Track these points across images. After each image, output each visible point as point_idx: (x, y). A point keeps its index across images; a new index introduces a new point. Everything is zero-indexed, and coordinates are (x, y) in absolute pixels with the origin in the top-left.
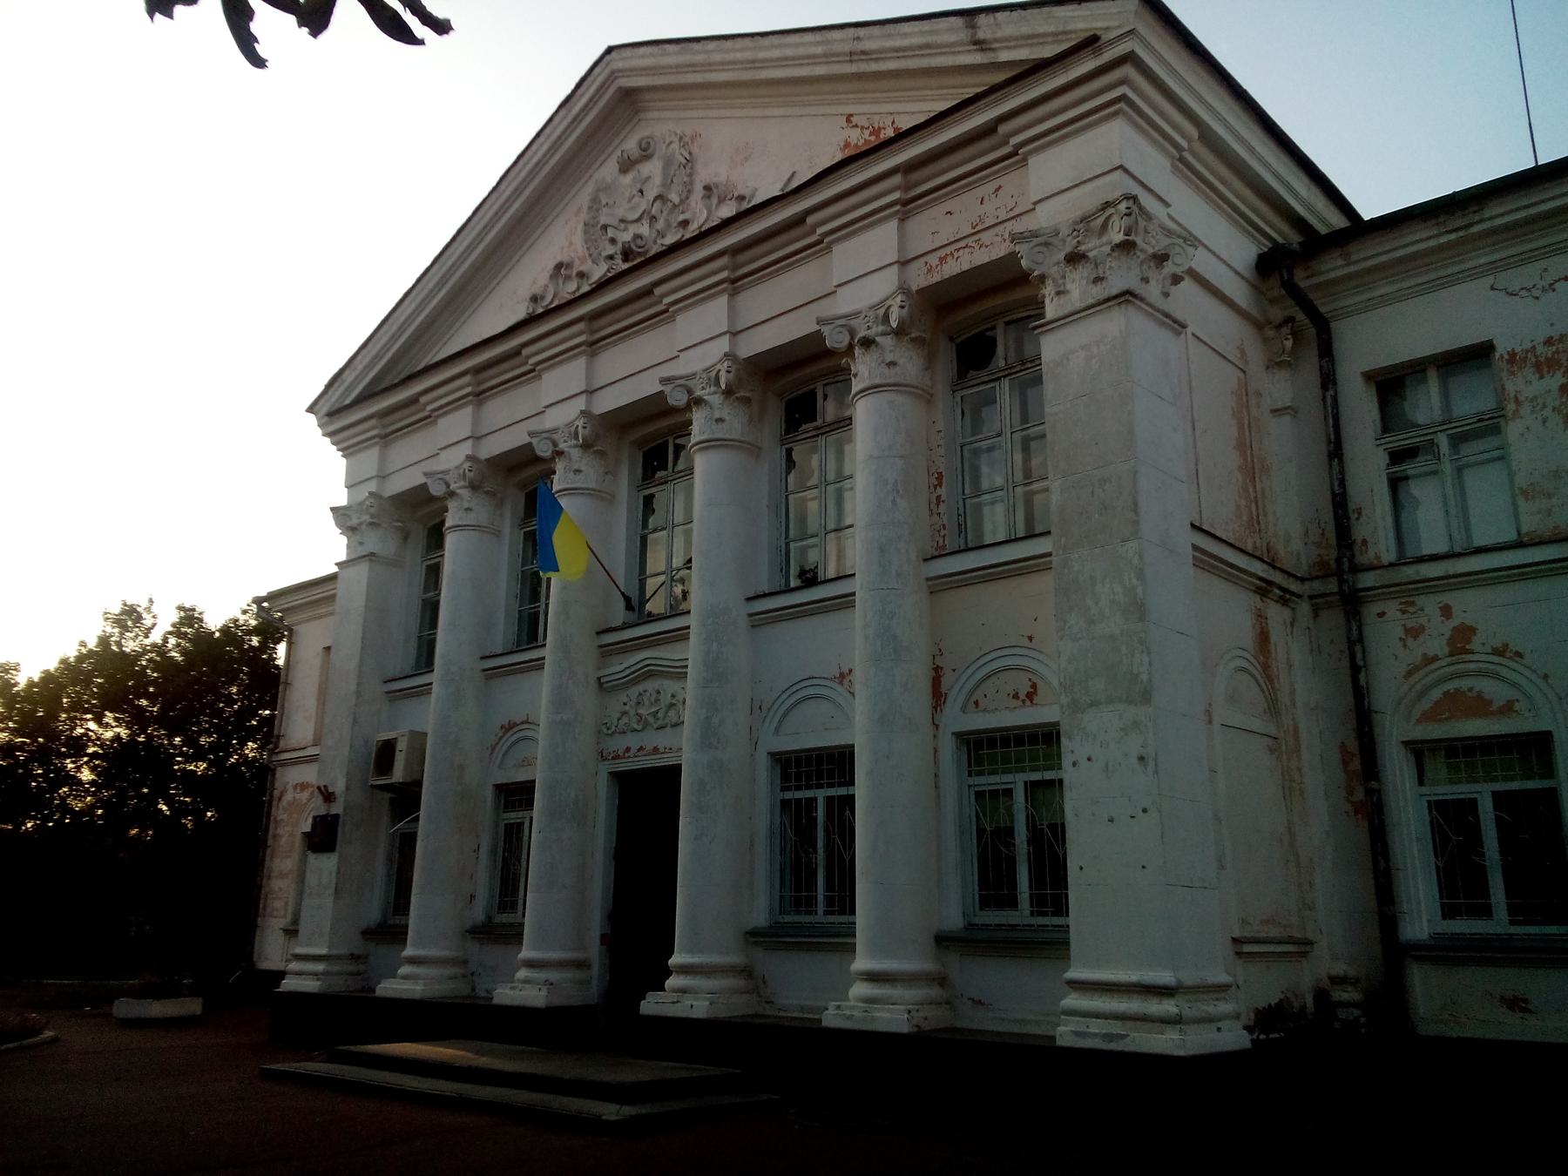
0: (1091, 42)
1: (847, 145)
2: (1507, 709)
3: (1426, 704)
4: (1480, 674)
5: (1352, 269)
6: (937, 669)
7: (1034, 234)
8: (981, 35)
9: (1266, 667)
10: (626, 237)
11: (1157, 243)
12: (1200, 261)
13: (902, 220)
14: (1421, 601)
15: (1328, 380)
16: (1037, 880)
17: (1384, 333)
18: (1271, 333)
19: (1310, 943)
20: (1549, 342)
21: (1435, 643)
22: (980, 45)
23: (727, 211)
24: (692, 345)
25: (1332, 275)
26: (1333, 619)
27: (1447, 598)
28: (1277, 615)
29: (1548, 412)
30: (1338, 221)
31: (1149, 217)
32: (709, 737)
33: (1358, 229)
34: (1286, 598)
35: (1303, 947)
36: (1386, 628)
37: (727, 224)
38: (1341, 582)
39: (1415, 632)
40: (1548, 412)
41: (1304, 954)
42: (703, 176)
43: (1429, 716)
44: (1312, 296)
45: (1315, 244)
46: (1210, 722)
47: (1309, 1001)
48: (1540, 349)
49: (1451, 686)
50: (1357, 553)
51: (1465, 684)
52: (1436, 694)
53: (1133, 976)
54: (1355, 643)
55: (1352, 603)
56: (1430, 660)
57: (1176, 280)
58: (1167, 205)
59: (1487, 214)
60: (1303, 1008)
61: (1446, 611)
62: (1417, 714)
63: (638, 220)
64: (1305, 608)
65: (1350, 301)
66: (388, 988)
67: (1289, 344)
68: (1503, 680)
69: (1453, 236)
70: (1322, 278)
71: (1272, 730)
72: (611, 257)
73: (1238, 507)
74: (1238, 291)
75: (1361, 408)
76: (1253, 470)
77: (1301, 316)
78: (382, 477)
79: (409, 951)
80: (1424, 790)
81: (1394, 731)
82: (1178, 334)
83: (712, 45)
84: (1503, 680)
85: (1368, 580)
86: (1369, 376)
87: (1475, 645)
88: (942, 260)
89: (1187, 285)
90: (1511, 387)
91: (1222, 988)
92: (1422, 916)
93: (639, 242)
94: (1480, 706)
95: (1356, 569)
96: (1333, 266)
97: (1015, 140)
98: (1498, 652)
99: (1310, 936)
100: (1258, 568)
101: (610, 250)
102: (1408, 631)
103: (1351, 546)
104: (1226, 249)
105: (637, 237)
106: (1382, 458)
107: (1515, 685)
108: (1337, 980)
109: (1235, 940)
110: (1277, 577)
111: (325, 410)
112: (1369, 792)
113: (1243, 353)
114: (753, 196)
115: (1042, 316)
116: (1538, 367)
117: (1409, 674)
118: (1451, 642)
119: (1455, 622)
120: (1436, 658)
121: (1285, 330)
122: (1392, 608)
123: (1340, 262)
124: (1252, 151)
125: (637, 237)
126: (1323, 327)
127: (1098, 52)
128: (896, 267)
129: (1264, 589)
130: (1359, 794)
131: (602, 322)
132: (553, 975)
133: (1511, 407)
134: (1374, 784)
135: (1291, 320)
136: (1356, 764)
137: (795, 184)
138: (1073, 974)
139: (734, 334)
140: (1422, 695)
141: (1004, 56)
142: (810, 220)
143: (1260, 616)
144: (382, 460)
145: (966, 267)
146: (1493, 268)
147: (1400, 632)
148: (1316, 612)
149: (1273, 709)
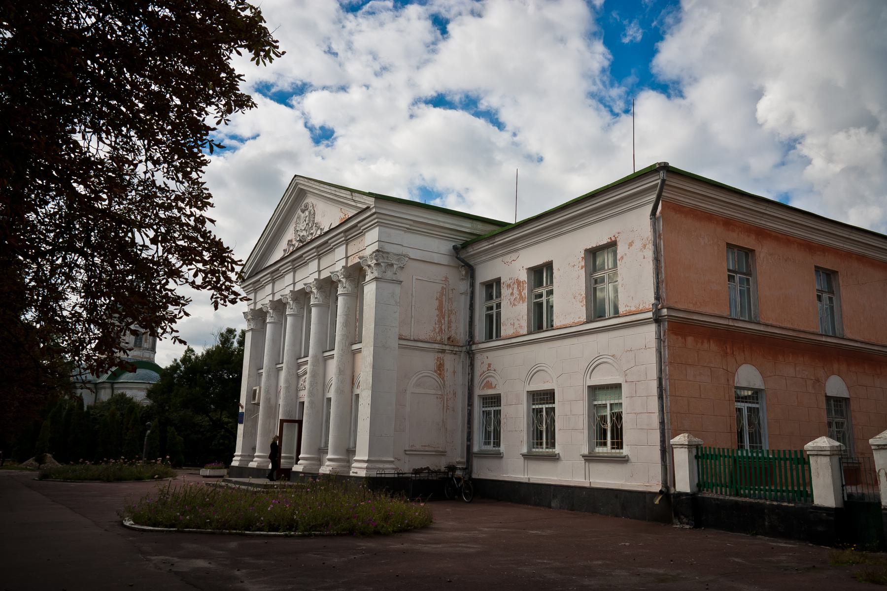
10: (302, 234)
13: (347, 245)
15: (472, 285)
16: (751, 440)
22: (354, 201)
32: (311, 394)
35: (442, 454)
37: (320, 236)
54: (472, 365)
55: (471, 355)
74: (445, 260)
81: (478, 392)
85: (474, 347)
91: (392, 462)
96: (471, 251)
106: (484, 309)
108: (459, 463)
141: (359, 205)
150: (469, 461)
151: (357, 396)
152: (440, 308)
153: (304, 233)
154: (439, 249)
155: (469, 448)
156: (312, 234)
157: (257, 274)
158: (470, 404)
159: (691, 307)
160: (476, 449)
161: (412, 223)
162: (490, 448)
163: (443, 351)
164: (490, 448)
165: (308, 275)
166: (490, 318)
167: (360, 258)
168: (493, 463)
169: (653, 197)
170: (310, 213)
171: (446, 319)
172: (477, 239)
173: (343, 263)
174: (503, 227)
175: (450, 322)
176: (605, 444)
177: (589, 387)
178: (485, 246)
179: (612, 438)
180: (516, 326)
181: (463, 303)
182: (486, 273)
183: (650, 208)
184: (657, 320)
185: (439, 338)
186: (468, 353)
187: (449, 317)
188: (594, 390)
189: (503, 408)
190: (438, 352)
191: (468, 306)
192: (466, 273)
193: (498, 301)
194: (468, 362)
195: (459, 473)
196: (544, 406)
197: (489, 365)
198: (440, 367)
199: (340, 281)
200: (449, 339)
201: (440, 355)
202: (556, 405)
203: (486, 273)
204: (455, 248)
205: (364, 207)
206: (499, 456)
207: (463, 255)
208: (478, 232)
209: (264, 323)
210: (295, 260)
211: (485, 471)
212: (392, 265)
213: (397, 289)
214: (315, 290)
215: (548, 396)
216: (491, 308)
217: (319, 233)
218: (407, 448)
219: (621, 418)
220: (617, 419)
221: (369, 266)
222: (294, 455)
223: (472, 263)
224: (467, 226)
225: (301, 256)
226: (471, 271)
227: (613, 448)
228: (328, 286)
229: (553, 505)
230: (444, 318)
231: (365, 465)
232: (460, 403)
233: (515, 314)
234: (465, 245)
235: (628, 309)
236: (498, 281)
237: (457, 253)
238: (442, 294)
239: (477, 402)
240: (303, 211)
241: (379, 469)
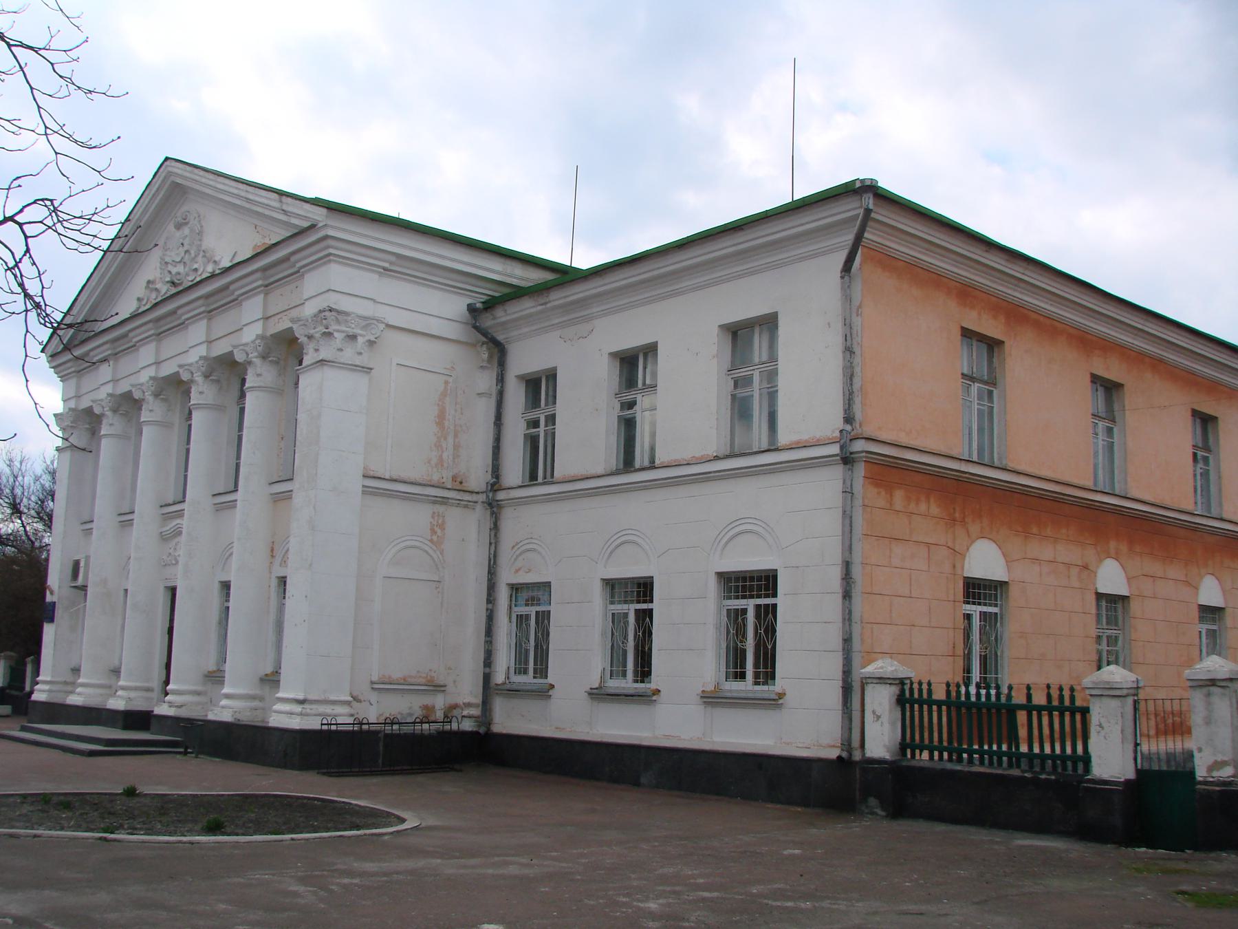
5: (508, 318)
7: (299, 320)
8: (285, 207)
10: (174, 271)
15: (501, 379)
22: (285, 212)
25: (503, 319)
35: (438, 688)
37: (213, 276)
53: (291, 696)
54: (495, 528)
55: (494, 508)
65: (515, 333)
66: (75, 699)
69: (540, 308)
75: (516, 396)
78: (78, 397)
79: (226, 690)
81: (507, 576)
83: (202, 173)
85: (501, 495)
86: (521, 377)
91: (348, 703)
96: (503, 315)
97: (298, 265)
109: (372, 683)
111: (50, 353)
128: (261, 322)
131: (162, 322)
132: (133, 694)
138: (280, 695)
139: (210, 342)
142: (232, 287)
144: (78, 387)
146: (562, 325)
150: (486, 704)
151: (283, 581)
152: (441, 419)
153: (180, 268)
154: (444, 309)
156: (196, 270)
158: (491, 598)
159: (904, 440)
160: (499, 678)
161: (393, 259)
162: (528, 679)
163: (444, 501)
164: (528, 679)
165: (190, 348)
166: (533, 442)
167: (293, 321)
168: (530, 706)
169: (849, 238)
171: (450, 440)
172: (517, 293)
173: (257, 329)
174: (564, 275)
175: (456, 447)
176: (741, 676)
178: (526, 306)
179: (756, 665)
181: (484, 411)
182: (527, 357)
183: (842, 256)
184: (847, 460)
186: (490, 504)
187: (456, 436)
190: (434, 502)
191: (493, 419)
192: (491, 357)
193: (549, 411)
194: (488, 524)
195: (467, 726)
198: (438, 527)
199: (250, 363)
200: (454, 478)
201: (440, 509)
202: (655, 606)
203: (527, 357)
204: (471, 309)
205: (306, 224)
207: (487, 321)
208: (515, 282)
209: (94, 432)
211: (512, 720)
212: (353, 337)
213: (362, 381)
214: (199, 378)
215: (644, 589)
216: (535, 423)
217: (210, 268)
218: (375, 679)
219: (774, 631)
220: (766, 631)
221: (310, 337)
222: (156, 683)
223: (500, 338)
224: (495, 269)
225: (174, 312)
226: (498, 351)
227: (756, 683)
228: (228, 370)
229: (643, 780)
230: (445, 439)
233: (584, 437)
234: (491, 305)
237: (475, 318)
238: (444, 394)
240: (179, 227)
241: (324, 715)
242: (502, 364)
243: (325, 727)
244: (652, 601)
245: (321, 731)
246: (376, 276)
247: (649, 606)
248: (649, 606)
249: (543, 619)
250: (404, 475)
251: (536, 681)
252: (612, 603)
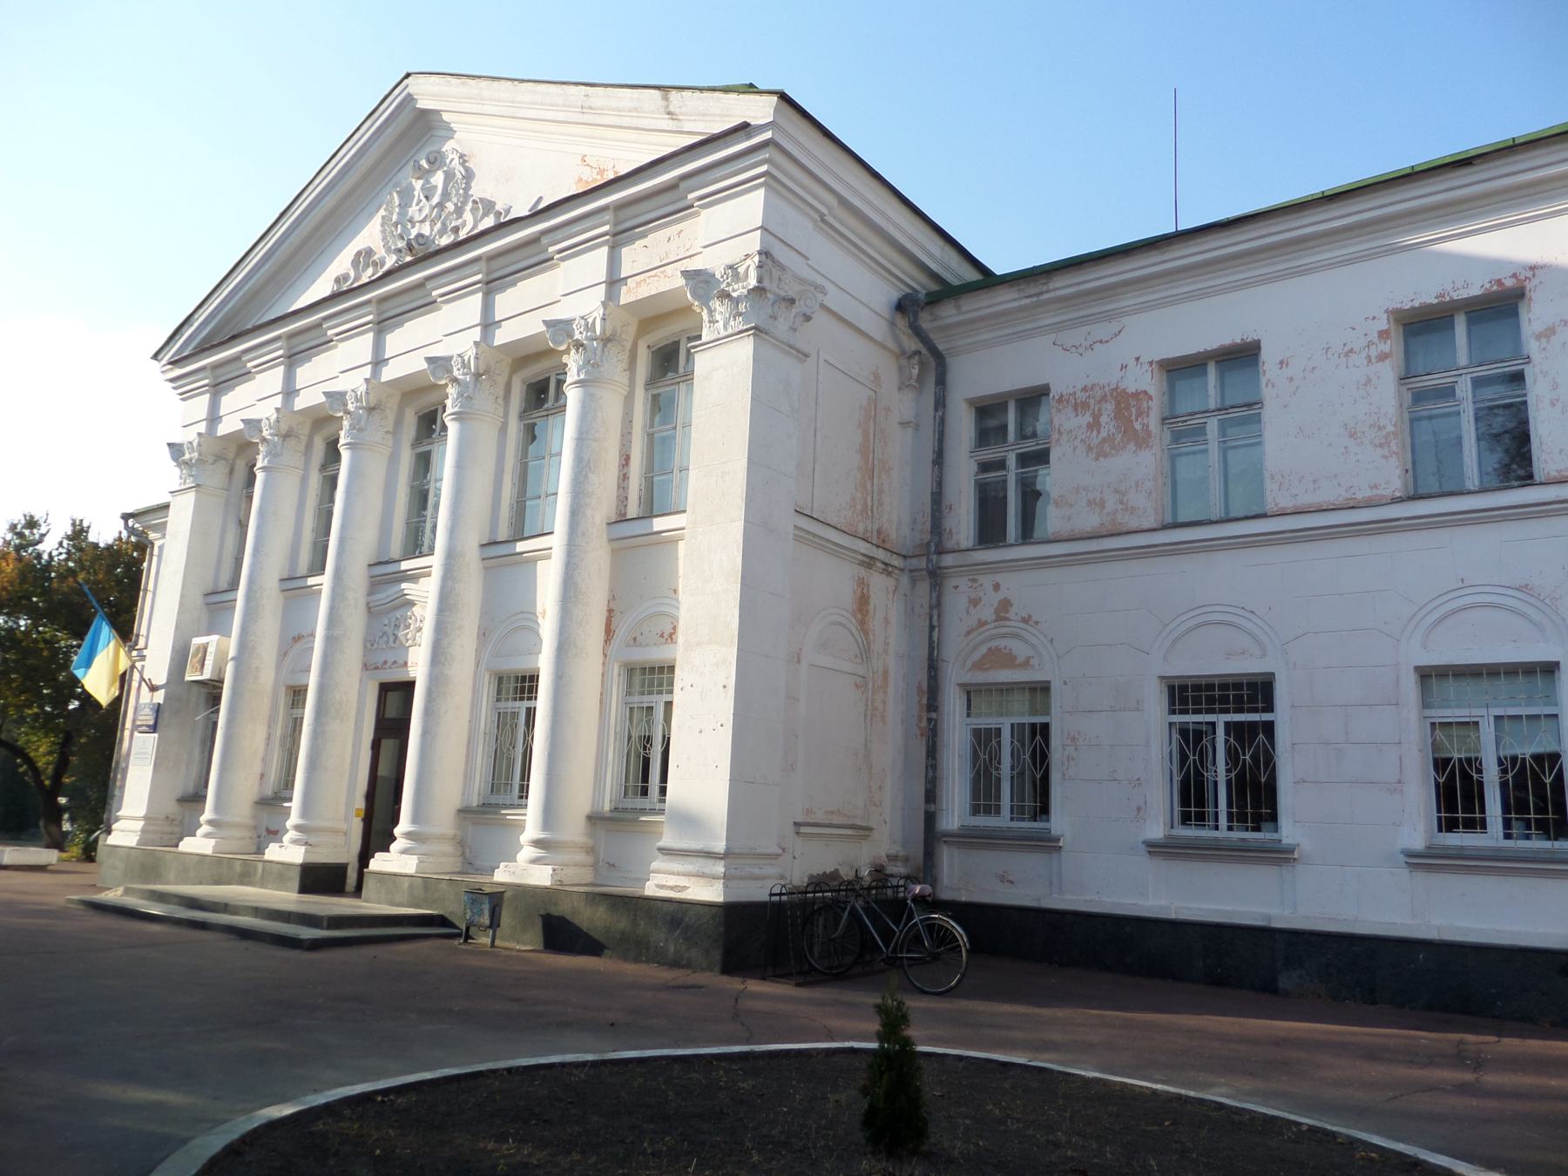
0: (744, 128)
1: (580, 180)
2: (1026, 664)
3: (977, 656)
4: (1015, 636)
5: (961, 318)
6: (610, 611)
8: (672, 109)
9: (862, 623)
11: (791, 290)
12: (833, 299)
14: (981, 579)
15: (940, 403)
17: (989, 369)
18: (904, 362)
19: (870, 829)
20: (1085, 389)
21: (987, 613)
23: (489, 222)
24: (446, 332)
25: (949, 321)
26: (924, 587)
27: (999, 578)
28: (880, 584)
29: (1077, 442)
30: (972, 275)
31: (782, 268)
33: (988, 280)
34: (887, 569)
35: (863, 832)
36: (957, 595)
38: (929, 560)
39: (975, 602)
40: (1077, 442)
41: (865, 837)
42: (477, 191)
43: (977, 666)
44: (932, 336)
45: (944, 292)
46: (799, 661)
47: (865, 872)
48: (1079, 394)
49: (989, 645)
50: (945, 537)
51: (1001, 643)
52: (983, 649)
54: (937, 605)
55: (936, 576)
56: (982, 624)
57: (808, 318)
58: (807, 258)
59: (1051, 286)
60: (858, 878)
61: (997, 587)
62: (969, 663)
63: (422, 221)
64: (905, 579)
67: (915, 372)
68: (1026, 641)
69: (1028, 301)
70: (940, 323)
71: (861, 670)
72: (400, 251)
73: (853, 499)
74: (879, 329)
75: (963, 426)
76: (870, 468)
77: (924, 351)
80: (969, 720)
81: (954, 676)
82: (802, 361)
84: (1026, 641)
85: (948, 560)
86: (971, 402)
87: (1011, 615)
88: (639, 283)
89: (820, 318)
90: (1056, 422)
92: (955, 812)
93: (421, 241)
94: (1008, 660)
95: (941, 551)
96: (949, 313)
98: (1026, 620)
99: (872, 824)
100: (862, 547)
101: (401, 244)
102: (970, 601)
103: (940, 535)
104: (865, 292)
105: (420, 235)
106: (974, 467)
107: (1033, 646)
108: (892, 858)
109: (796, 824)
110: (880, 554)
112: (929, 720)
113: (876, 377)
114: (508, 211)
115: (700, 337)
116: (1075, 407)
117: (968, 633)
118: (997, 612)
119: (1001, 596)
120: (986, 623)
121: (915, 360)
122: (963, 583)
123: (954, 311)
124: (889, 219)
125: (420, 235)
126: (940, 358)
127: (749, 137)
129: (869, 562)
130: (924, 724)
133: (1056, 436)
134: (934, 715)
135: (918, 353)
136: (925, 701)
137: (541, 206)
140: (975, 648)
141: (687, 127)
143: (862, 583)
145: (653, 292)
146: (1057, 327)
147: (965, 600)
148: (914, 581)
149: (865, 653)
152: (864, 451)
155: (930, 819)
157: (235, 338)
170: (449, 176)
177: (1417, 669)
180: (1111, 505)
185: (861, 528)
188: (1428, 676)
189: (1283, 716)
192: (921, 378)
196: (1221, 720)
197: (1005, 605)
200: (879, 532)
201: (863, 572)
206: (1048, 844)
207: (925, 321)
210: (391, 299)
226: (932, 364)
229: (1285, 981)
231: (720, 868)
232: (897, 704)
235: (1375, 492)
236: (1032, 399)
239: (953, 703)
242: (941, 381)
243: (776, 898)
244: (1270, 708)
245: (773, 904)
246: (810, 225)
247: (1266, 717)
248: (1266, 717)
249: (1042, 732)
250: (832, 520)
251: (1015, 824)
252: (1173, 712)
